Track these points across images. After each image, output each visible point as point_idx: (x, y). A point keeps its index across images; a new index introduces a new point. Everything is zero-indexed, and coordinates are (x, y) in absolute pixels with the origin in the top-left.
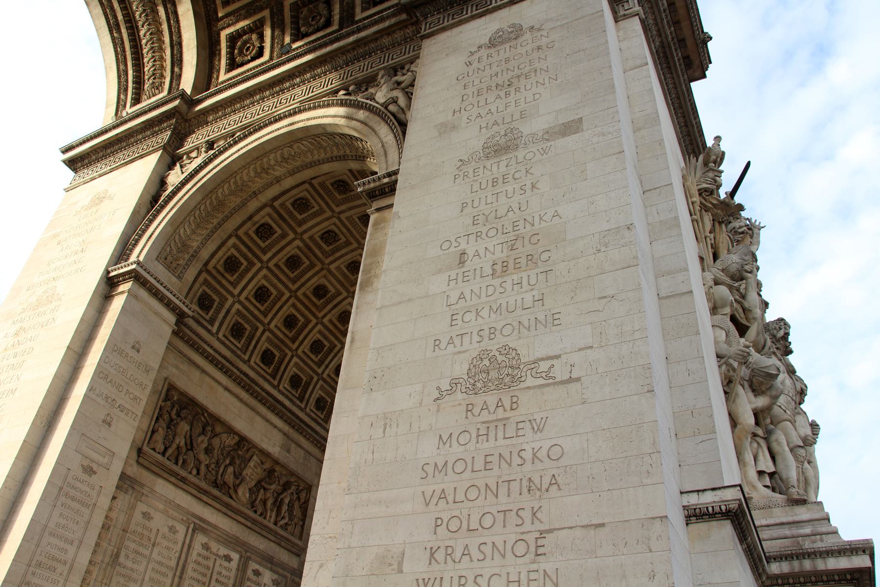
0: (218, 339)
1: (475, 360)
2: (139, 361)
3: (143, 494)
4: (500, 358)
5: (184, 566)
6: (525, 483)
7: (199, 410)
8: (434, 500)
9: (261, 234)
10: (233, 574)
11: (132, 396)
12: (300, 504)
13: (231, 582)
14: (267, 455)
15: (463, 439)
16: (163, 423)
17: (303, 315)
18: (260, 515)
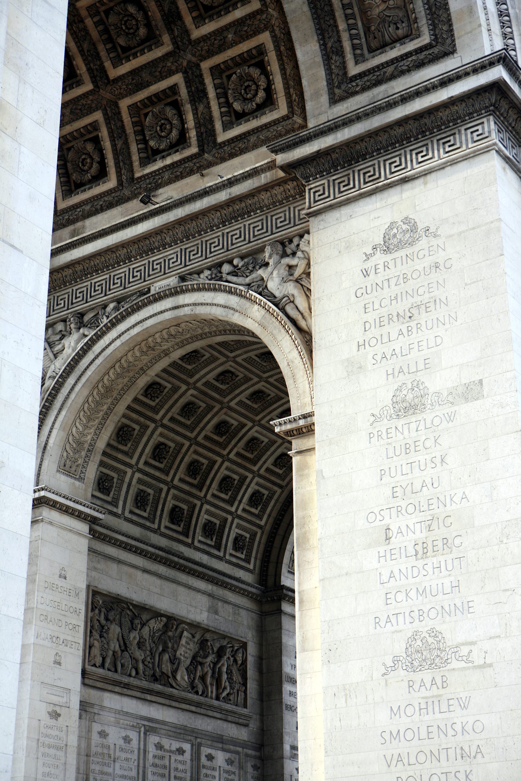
0: (127, 520)
1: (410, 640)
2: (69, 588)
3: (95, 713)
4: (430, 640)
5: (144, 772)
6: (459, 751)
7: (124, 605)
8: (394, 762)
9: (151, 395)
10: (188, 767)
11: (71, 627)
12: (238, 666)
13: (189, 774)
14: (194, 626)
15: (410, 711)
16: (96, 635)
17: (205, 458)
18: (201, 695)
